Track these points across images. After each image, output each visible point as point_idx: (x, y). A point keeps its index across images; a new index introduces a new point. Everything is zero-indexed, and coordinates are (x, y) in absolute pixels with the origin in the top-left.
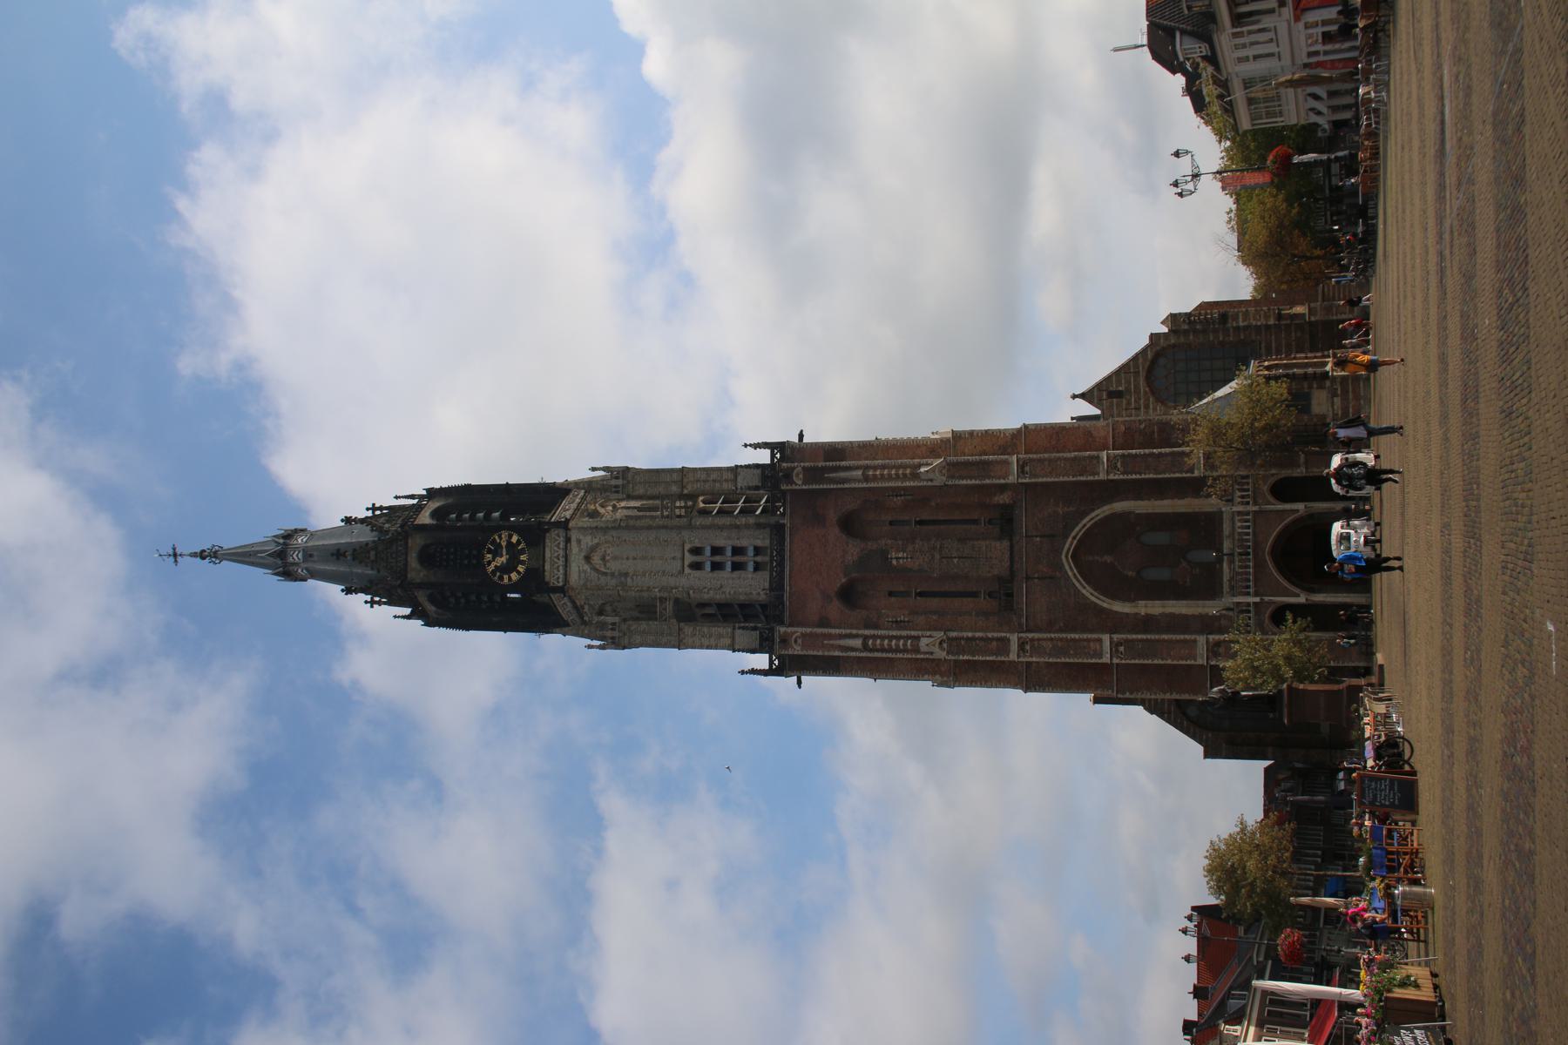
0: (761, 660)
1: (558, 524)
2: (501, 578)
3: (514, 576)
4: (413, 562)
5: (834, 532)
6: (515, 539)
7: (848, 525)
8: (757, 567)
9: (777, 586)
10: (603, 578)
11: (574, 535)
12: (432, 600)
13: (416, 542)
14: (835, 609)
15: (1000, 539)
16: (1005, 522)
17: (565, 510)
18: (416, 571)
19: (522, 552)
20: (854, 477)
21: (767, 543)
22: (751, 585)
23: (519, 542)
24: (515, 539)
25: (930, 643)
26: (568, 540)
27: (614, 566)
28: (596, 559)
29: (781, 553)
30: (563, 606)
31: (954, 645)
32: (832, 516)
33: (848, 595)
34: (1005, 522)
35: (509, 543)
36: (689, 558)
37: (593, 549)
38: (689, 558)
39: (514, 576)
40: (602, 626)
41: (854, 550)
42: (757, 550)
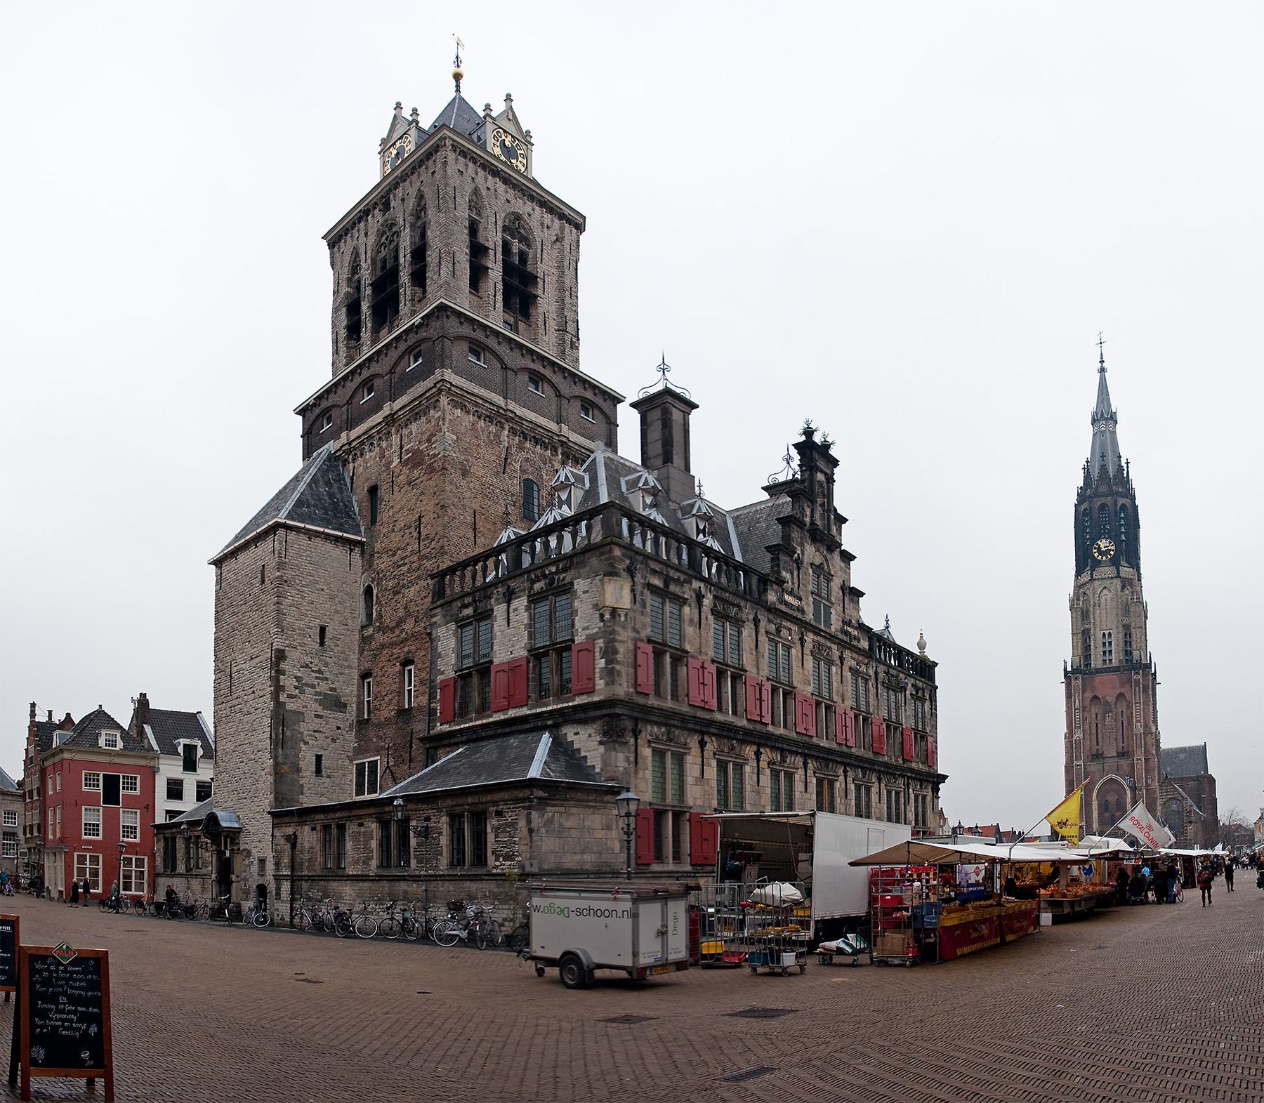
0: (1069, 669)
1: (1118, 573)
2: (1095, 548)
3: (1096, 555)
4: (1103, 500)
5: (1118, 691)
6: (1112, 553)
7: (1121, 695)
8: (1105, 661)
9: (1098, 671)
10: (1097, 596)
11: (1115, 581)
12: (1085, 509)
13: (1109, 500)
14: (1089, 695)
15: (1117, 752)
16: (1123, 754)
17: (1126, 571)
18: (1098, 502)
19: (1107, 557)
20: (1137, 697)
21: (1114, 665)
22: (1096, 662)
23: (1110, 555)
24: (1112, 553)
25: (1078, 735)
26: (1112, 578)
27: (1103, 600)
28: (1105, 592)
29: (1110, 671)
30: (1085, 577)
31: (1078, 742)
32: (1123, 690)
33: (1095, 697)
34: (1123, 754)
35: (1110, 550)
36: (1107, 632)
37: (1109, 590)
38: (1107, 632)
39: (1096, 555)
40: (1078, 599)
41: (1111, 699)
42: (1110, 660)
